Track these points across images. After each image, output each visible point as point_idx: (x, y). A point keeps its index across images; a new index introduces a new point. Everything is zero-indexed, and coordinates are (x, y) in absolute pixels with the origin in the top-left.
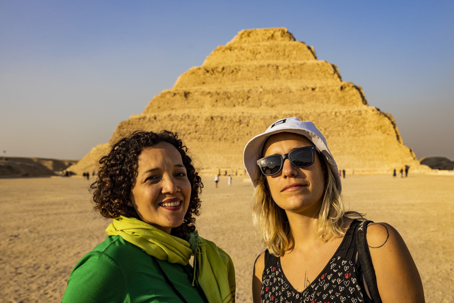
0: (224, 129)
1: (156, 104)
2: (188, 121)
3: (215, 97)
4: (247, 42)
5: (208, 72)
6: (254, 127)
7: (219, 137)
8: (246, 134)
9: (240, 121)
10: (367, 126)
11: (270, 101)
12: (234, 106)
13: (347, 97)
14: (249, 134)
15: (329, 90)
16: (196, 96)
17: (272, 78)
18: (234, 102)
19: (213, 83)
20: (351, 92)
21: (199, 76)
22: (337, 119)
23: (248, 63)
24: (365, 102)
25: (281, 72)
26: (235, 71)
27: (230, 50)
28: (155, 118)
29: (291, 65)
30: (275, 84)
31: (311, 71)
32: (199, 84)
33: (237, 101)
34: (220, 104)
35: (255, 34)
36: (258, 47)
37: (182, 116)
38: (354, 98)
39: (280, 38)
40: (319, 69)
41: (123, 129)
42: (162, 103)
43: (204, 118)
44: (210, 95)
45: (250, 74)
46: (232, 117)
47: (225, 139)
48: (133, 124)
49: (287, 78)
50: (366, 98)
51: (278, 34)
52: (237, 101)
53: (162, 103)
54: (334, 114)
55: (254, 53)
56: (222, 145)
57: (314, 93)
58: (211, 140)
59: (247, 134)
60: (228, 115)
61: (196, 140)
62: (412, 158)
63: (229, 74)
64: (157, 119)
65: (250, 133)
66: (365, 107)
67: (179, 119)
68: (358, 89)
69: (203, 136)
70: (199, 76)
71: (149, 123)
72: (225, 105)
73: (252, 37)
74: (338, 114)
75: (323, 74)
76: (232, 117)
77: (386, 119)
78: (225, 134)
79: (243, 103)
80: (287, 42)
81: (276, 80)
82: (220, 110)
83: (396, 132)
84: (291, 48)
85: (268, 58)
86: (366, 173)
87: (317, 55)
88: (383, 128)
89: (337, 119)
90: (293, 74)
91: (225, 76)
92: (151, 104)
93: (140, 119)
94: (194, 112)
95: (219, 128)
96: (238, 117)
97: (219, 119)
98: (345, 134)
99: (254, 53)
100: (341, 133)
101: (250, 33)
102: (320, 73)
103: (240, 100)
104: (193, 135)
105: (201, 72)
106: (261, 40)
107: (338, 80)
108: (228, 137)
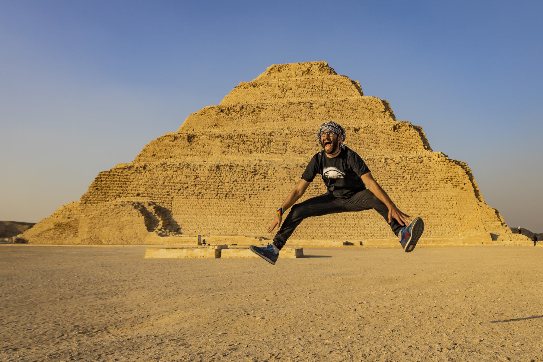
0: (234, 182)
1: (150, 151)
2: (186, 171)
3: (227, 141)
4: (277, 78)
5: (222, 111)
6: (274, 178)
7: (225, 193)
8: (261, 188)
9: (255, 171)
10: (431, 177)
11: (298, 146)
12: (251, 152)
13: (402, 140)
14: (266, 189)
15: (377, 131)
16: (203, 140)
17: (303, 117)
18: (250, 148)
19: (228, 125)
20: (407, 133)
21: (211, 116)
22: (388, 168)
23: (274, 101)
25: (315, 109)
26: (256, 110)
27: (254, 86)
28: (145, 168)
29: (329, 102)
31: (354, 109)
33: (256, 146)
34: (232, 150)
35: (287, 69)
36: (289, 82)
37: (180, 164)
38: (412, 141)
39: (318, 73)
40: (366, 105)
41: (102, 181)
42: (158, 150)
43: (208, 167)
44: (220, 138)
45: (276, 114)
46: (245, 166)
47: (233, 195)
48: (114, 175)
50: (430, 141)
51: (317, 68)
52: (256, 146)
53: (158, 150)
54: (383, 161)
55: (284, 90)
56: (229, 203)
57: (357, 135)
58: (214, 196)
59: (264, 189)
60: (241, 163)
61: (194, 196)
62: (500, 223)
63: (249, 114)
64: (147, 169)
65: (267, 187)
66: (428, 153)
67: (175, 169)
68: (418, 129)
69: (204, 190)
70: (211, 116)
71: (136, 173)
72: (239, 151)
73: (283, 73)
74: (389, 161)
75: (371, 112)
76: (245, 166)
77: (458, 166)
78: (234, 189)
79: (263, 149)
80: (326, 76)
81: (308, 121)
82: (234, 158)
83: (473, 185)
84: (331, 83)
86: (431, 244)
87: (363, 91)
88: (454, 180)
89: (388, 168)
90: (330, 113)
91: (243, 117)
92: (144, 150)
93: (125, 169)
94: (197, 160)
95: (227, 181)
96: (252, 166)
97: (228, 168)
98: (400, 188)
100: (393, 187)
101: (281, 67)
102: (366, 111)
103: (259, 145)
104: (190, 190)
105: (213, 112)
106: (294, 75)
107: (391, 119)
108: (237, 193)
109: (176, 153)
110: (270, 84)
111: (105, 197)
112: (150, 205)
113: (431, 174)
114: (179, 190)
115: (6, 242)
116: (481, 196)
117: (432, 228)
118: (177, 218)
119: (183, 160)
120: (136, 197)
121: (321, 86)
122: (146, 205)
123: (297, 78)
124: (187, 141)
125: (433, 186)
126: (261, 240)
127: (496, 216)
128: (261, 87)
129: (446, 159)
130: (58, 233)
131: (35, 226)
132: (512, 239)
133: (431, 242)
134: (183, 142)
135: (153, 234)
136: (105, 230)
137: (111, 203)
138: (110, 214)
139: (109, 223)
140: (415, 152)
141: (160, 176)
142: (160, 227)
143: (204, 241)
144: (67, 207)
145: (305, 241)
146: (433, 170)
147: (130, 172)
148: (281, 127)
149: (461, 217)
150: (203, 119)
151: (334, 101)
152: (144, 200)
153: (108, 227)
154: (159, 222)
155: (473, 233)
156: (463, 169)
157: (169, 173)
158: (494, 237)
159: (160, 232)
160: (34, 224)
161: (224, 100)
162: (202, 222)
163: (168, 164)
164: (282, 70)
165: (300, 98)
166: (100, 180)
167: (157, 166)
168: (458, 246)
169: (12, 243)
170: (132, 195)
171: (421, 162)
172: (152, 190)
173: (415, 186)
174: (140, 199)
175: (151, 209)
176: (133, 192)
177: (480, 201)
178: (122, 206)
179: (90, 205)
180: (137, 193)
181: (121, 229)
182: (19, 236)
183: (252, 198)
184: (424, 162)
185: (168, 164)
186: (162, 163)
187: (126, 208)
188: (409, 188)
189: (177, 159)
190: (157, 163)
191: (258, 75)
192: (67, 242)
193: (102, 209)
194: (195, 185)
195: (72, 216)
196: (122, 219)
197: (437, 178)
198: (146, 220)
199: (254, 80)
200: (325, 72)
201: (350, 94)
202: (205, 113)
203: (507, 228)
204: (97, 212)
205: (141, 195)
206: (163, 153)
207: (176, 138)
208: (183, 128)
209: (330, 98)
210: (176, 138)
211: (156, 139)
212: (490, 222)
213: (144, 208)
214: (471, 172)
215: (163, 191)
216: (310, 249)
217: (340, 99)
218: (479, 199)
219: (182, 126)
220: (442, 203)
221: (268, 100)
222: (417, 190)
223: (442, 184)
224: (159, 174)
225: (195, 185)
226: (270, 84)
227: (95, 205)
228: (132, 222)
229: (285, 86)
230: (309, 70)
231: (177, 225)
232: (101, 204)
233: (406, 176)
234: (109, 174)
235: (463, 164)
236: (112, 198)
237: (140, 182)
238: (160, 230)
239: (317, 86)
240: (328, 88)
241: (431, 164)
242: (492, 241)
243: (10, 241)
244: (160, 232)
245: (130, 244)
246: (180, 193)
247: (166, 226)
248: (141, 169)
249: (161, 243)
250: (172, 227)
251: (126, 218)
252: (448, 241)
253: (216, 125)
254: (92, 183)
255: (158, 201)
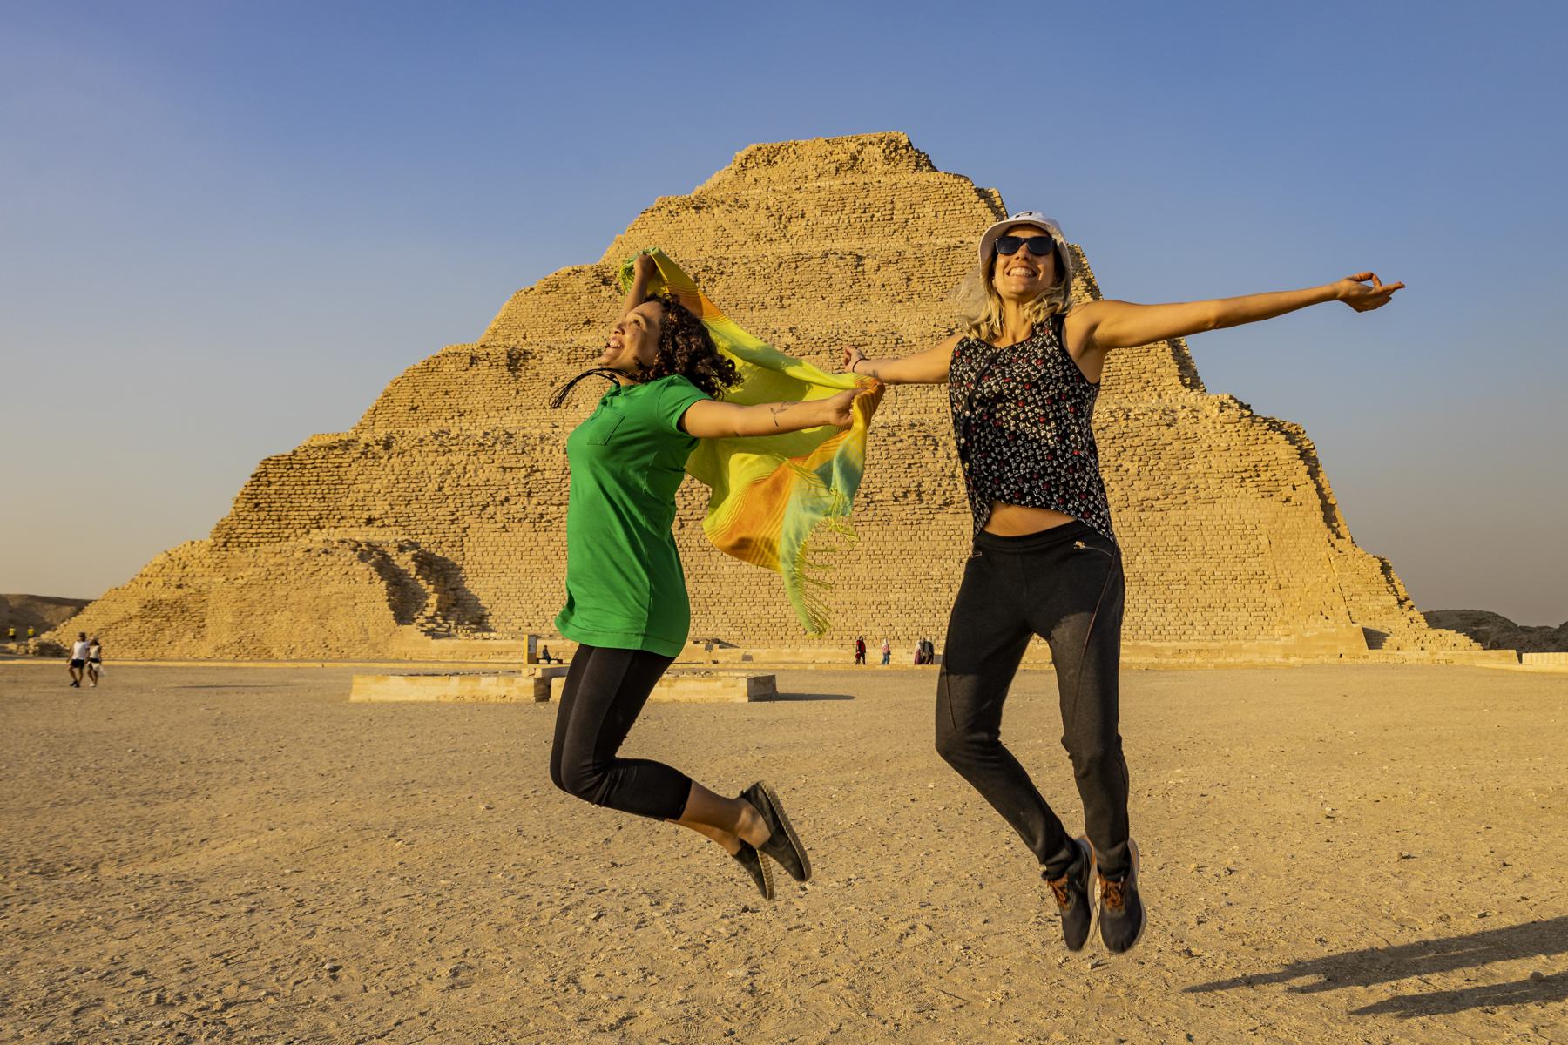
1: (405, 396)
2: (503, 454)
4: (764, 182)
5: (606, 282)
10: (1197, 467)
21: (576, 297)
24: (1190, 377)
25: (870, 274)
29: (910, 251)
30: (849, 319)
32: (572, 327)
35: (793, 156)
36: (797, 196)
37: (486, 434)
39: (881, 167)
41: (270, 483)
42: (424, 393)
45: (758, 287)
48: (303, 466)
49: (896, 299)
50: (1198, 363)
51: (877, 151)
53: (424, 393)
55: (781, 218)
61: (526, 526)
64: (395, 447)
66: (1191, 397)
67: (472, 449)
80: (907, 176)
81: (849, 307)
83: (1319, 489)
85: (831, 231)
90: (914, 284)
92: (387, 395)
99: (781, 218)
101: (777, 152)
104: (514, 508)
105: (579, 284)
109: (475, 402)
110: (742, 200)
111: (280, 527)
112: (402, 549)
113: (1199, 459)
114: (484, 508)
115: (11, 655)
116: (1341, 520)
117: (1198, 615)
118: (479, 586)
119: (494, 422)
120: (364, 528)
121: (888, 206)
122: (392, 551)
123: (822, 183)
124: (505, 369)
125: (1202, 494)
126: (709, 648)
127: (1383, 578)
128: (716, 211)
129: (1242, 416)
130: (152, 629)
131: (88, 609)
132: (1426, 644)
133: (1193, 654)
134: (493, 371)
135: (412, 633)
136: (280, 620)
137: (297, 544)
138: (292, 577)
139: (290, 601)
140: (1155, 394)
141: (431, 470)
142: (429, 612)
143: (545, 651)
144: (175, 556)
145: (834, 650)
146: (1205, 446)
147: (347, 458)
148: (773, 326)
149: (1283, 581)
150: (551, 306)
151: (926, 249)
152: (387, 537)
153: (287, 613)
154: (427, 597)
155: (1316, 627)
156: (1292, 443)
157: (454, 459)
158: (1374, 639)
159: (430, 625)
160: (87, 602)
161: (611, 250)
162: (548, 597)
163: (453, 434)
164: (778, 159)
165: (828, 242)
166: (263, 479)
167: (421, 440)
168: (1267, 668)
169: (26, 655)
170: (353, 521)
171: (1169, 425)
172: (408, 510)
173: (1150, 493)
174: (375, 535)
175: (404, 561)
176: (357, 514)
177: (1338, 537)
178: (326, 552)
179: (237, 551)
180: (366, 515)
181: (323, 617)
182: (46, 637)
183: (687, 531)
184: (1180, 423)
185: (453, 434)
186: (436, 430)
187: (335, 558)
188: (1133, 500)
189: (479, 420)
190: (423, 431)
191: (709, 176)
192: (175, 653)
193: (272, 561)
194: (529, 494)
195: (188, 580)
196: (326, 590)
197: (1213, 470)
198: (390, 593)
199: (699, 189)
200: (903, 165)
201: (973, 228)
202: (557, 287)
203: (1415, 613)
204: (258, 570)
205: (379, 523)
206: (439, 402)
207: (474, 360)
208: (495, 332)
209: (914, 242)
210: (474, 360)
211: (419, 365)
212: (1365, 597)
213: (386, 557)
214: (1313, 453)
215: (440, 511)
216: (835, 674)
217: (941, 242)
218: (1334, 530)
219: (494, 325)
220: (1227, 542)
221: (736, 247)
222: (1157, 505)
223: (1228, 489)
224: (428, 463)
225: (529, 494)
226: (742, 200)
227: (251, 550)
228: (354, 597)
229: (785, 206)
230: (855, 158)
231: (479, 607)
232: (268, 548)
233: (1127, 465)
234: (290, 463)
235: (1293, 430)
236: (299, 532)
237: (374, 484)
238: (431, 619)
239: (879, 204)
240: (908, 211)
241: (1199, 429)
242: (1366, 651)
243: (22, 649)
244: (430, 625)
245: (347, 659)
246: (485, 515)
247: (448, 610)
248: (377, 448)
249: (434, 657)
250: (465, 612)
251: (335, 586)
252: (1240, 650)
253: (588, 322)
254: (241, 489)
255: (424, 538)
